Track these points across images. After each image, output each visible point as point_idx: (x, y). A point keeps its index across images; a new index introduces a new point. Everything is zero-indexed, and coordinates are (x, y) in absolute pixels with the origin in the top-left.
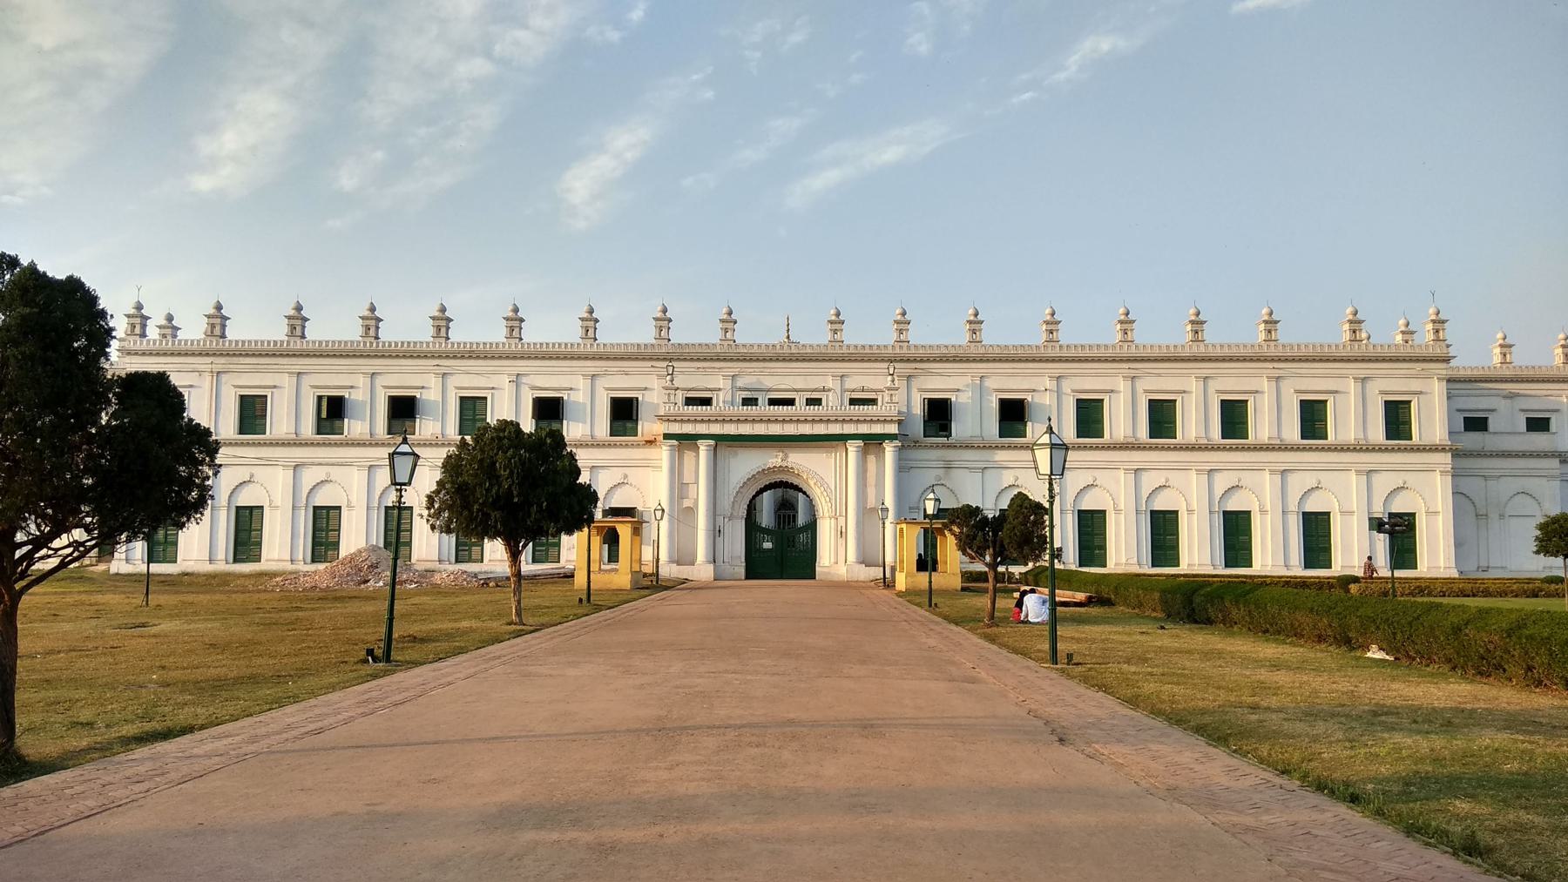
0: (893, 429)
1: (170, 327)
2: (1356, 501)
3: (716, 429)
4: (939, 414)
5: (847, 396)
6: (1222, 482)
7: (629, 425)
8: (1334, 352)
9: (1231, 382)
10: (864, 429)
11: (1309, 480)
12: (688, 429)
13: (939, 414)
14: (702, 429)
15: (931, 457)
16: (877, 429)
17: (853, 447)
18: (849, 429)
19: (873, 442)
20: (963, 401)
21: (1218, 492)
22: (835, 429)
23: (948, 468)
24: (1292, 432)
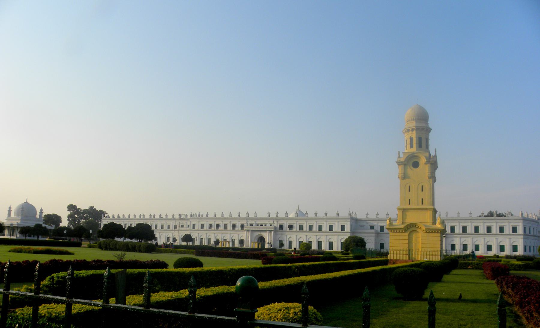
0: (273, 229)
1: (202, 216)
2: (336, 240)
3: (251, 229)
4: (281, 227)
5: (270, 224)
6: (318, 237)
7: (292, 229)
8: (334, 218)
9: (331, 222)
10: (269, 229)
11: (330, 237)
12: (248, 229)
13: (281, 227)
14: (250, 229)
15: (279, 233)
16: (271, 229)
17: (268, 231)
18: (267, 229)
19: (270, 231)
20: (295, 225)
21: (317, 239)
22: (266, 229)
23: (282, 234)
24: (340, 230)
